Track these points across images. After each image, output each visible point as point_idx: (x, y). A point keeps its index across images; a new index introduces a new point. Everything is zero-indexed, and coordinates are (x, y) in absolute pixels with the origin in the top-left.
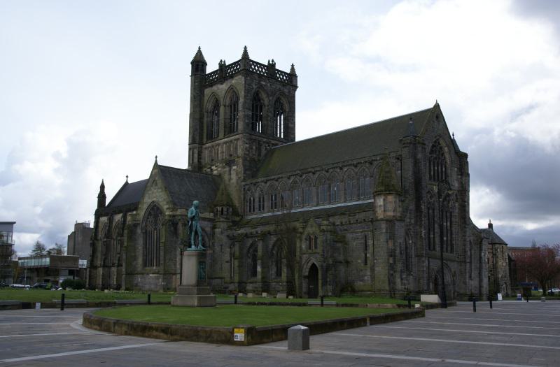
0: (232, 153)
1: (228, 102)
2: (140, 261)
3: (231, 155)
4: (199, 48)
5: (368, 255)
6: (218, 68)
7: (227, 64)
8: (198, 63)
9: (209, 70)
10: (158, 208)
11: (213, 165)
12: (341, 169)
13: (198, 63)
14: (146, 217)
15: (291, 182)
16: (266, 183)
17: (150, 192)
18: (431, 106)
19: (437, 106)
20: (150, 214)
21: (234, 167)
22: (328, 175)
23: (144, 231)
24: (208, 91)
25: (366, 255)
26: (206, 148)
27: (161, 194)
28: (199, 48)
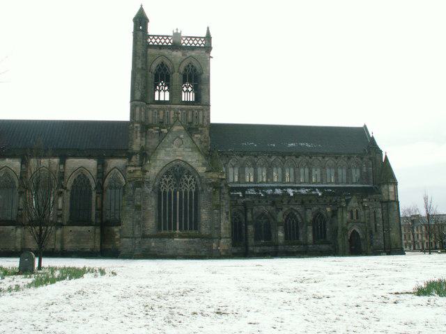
0: (190, 121)
1: (182, 70)
2: (151, 223)
3: (189, 123)
4: (142, 6)
5: (378, 225)
6: (172, 34)
7: (182, 35)
8: (141, 21)
9: (152, 29)
10: (182, 169)
11: (164, 128)
12: (323, 158)
13: (141, 21)
14: (159, 177)
15: (272, 160)
16: (242, 157)
17: (168, 149)
18: (362, 126)
19: (365, 126)
20: (167, 173)
21: (196, 136)
22: (310, 160)
23: (156, 190)
24: (150, 51)
25: (376, 225)
26: (150, 109)
27: (190, 153)
28: (142, 6)
